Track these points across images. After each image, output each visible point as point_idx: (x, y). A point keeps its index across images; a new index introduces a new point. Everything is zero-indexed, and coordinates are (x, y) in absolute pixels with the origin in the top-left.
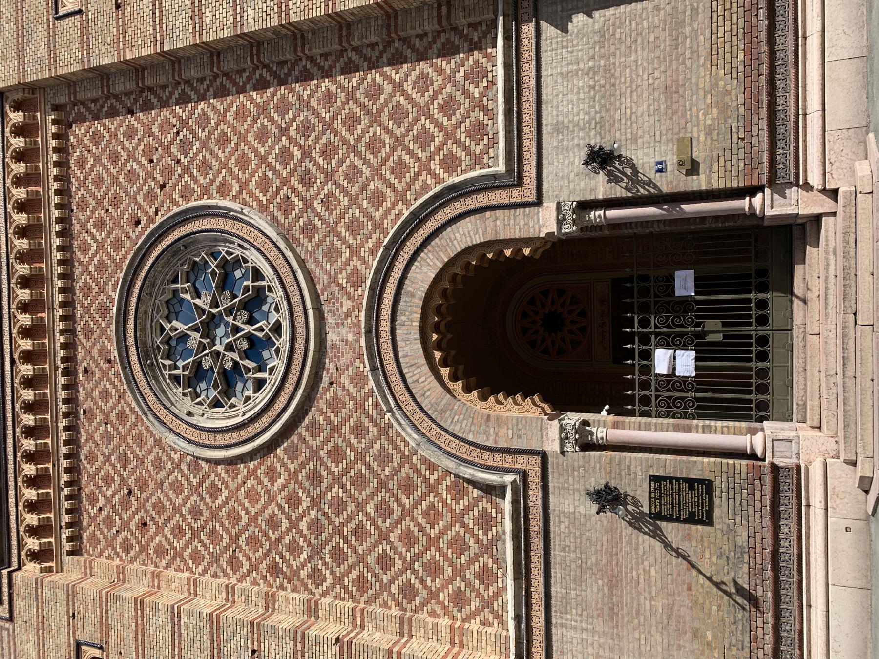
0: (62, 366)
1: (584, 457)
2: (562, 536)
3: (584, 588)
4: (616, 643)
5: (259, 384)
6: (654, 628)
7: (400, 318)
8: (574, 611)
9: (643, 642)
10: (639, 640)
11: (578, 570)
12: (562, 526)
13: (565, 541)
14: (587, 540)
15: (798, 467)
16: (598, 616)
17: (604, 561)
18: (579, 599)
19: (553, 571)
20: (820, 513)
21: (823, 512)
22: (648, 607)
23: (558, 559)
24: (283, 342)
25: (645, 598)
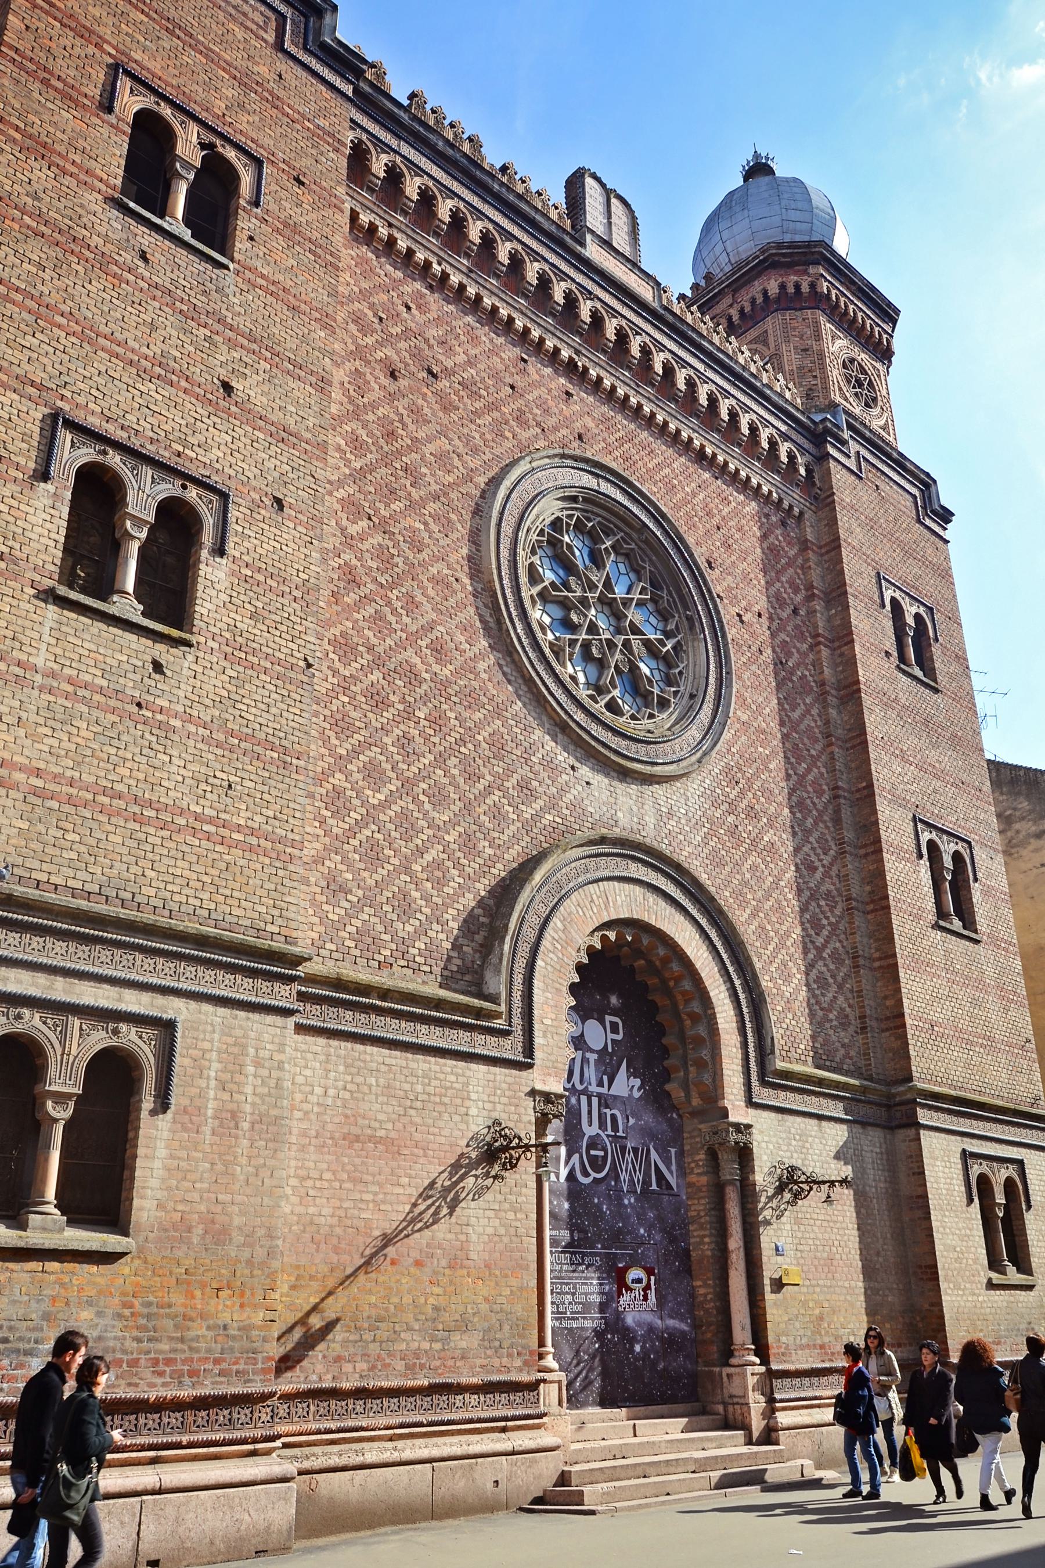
0: (580, 364)
1: (529, 1122)
2: (442, 1076)
3: (380, 1099)
4: (313, 1141)
5: (557, 652)
6: (338, 1204)
7: (652, 898)
8: (349, 1078)
9: (318, 1184)
10: (321, 1179)
11: (402, 1093)
12: (453, 1078)
13: (436, 1078)
14: (440, 1113)
15: (540, 1416)
16: (346, 1117)
17: (418, 1136)
18: (366, 1089)
19: (397, 1053)
20: (507, 1446)
21: (510, 1448)
22: (366, 1197)
23: (414, 1065)
24: (599, 707)
25: (375, 1194)
